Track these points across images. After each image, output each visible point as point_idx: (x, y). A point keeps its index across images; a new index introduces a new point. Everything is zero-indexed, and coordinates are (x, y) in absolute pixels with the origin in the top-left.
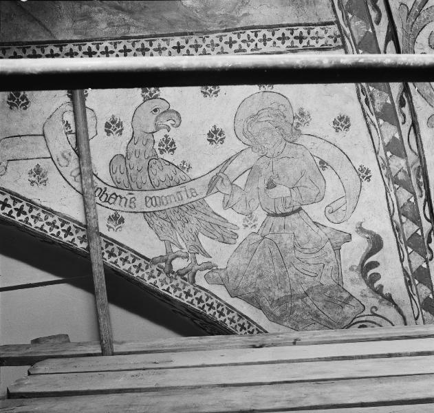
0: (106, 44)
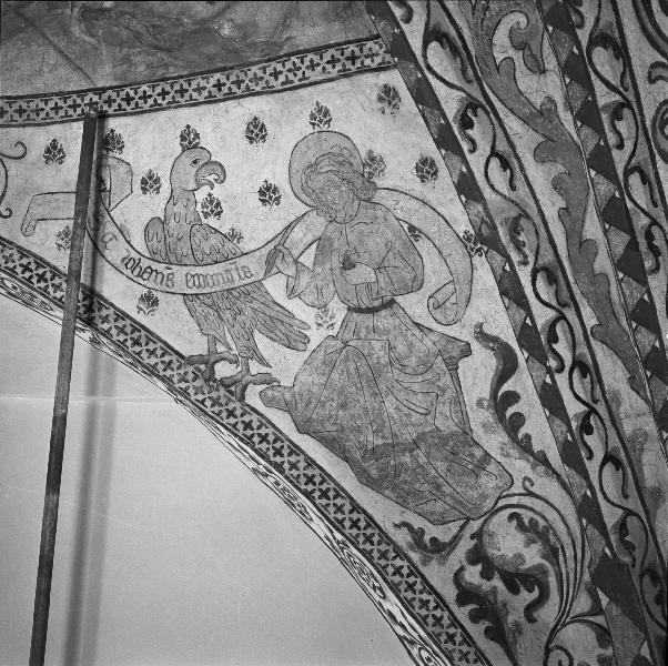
0: (144, 87)
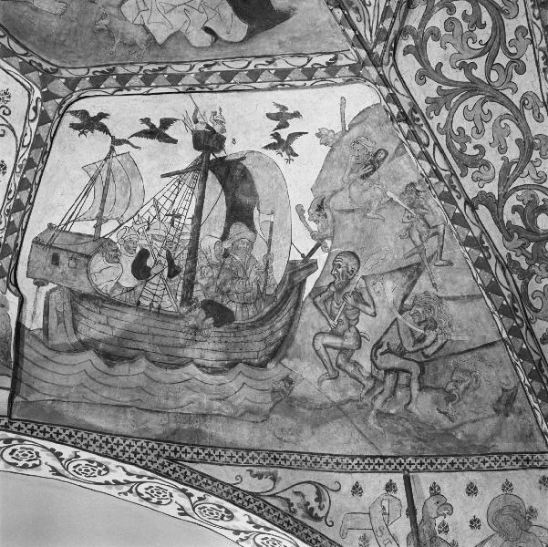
0: (410, 459)
